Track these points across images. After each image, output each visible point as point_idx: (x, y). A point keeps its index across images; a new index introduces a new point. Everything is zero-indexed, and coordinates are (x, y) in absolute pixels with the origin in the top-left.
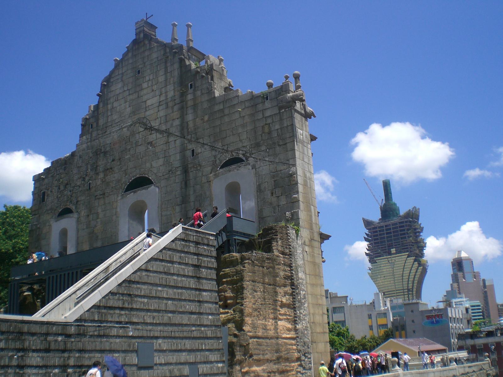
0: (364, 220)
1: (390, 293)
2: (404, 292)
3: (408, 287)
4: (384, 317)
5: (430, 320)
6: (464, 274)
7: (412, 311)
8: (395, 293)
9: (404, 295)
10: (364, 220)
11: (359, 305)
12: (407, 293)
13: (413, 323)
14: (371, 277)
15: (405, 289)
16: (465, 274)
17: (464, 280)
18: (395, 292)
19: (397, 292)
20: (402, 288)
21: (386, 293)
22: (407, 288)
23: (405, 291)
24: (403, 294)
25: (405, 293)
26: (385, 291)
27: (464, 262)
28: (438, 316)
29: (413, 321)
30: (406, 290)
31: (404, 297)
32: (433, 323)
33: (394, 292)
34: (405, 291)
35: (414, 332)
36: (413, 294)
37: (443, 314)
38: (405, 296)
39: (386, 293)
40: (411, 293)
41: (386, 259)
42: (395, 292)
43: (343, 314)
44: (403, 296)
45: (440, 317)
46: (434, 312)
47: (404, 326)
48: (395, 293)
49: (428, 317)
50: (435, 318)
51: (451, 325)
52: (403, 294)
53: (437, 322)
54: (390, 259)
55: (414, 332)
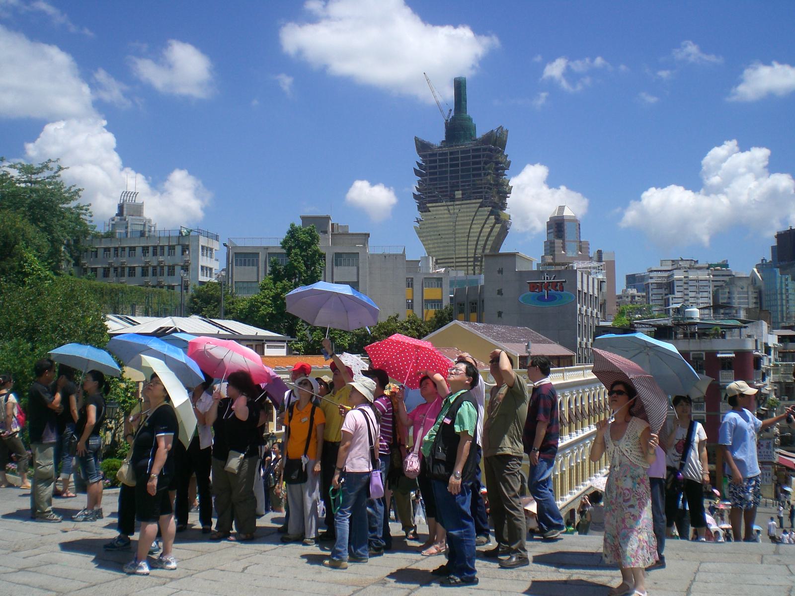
0: (417, 140)
1: (447, 261)
2: (468, 262)
3: (475, 254)
4: (438, 287)
5: (536, 293)
6: (563, 243)
7: (501, 271)
8: (453, 262)
9: (468, 266)
10: (417, 140)
11: (390, 255)
12: (472, 264)
13: (499, 296)
14: (418, 233)
15: (470, 257)
16: (567, 243)
17: (563, 252)
18: (454, 260)
19: (458, 260)
20: (466, 256)
22: (473, 255)
23: (469, 260)
24: (466, 264)
25: (469, 264)
27: (566, 223)
28: (555, 285)
29: (500, 292)
30: (472, 259)
31: (468, 270)
32: (541, 299)
33: (451, 260)
34: (469, 260)
35: (500, 314)
36: (481, 266)
37: (565, 282)
38: (469, 268)
40: (479, 264)
41: (446, 208)
42: (454, 260)
43: (355, 268)
44: (466, 268)
45: (558, 288)
46: (546, 276)
47: (476, 304)
48: (453, 262)
49: (533, 287)
50: (547, 288)
51: (579, 306)
52: (466, 264)
53: (551, 298)
54: (451, 207)
55: (500, 314)
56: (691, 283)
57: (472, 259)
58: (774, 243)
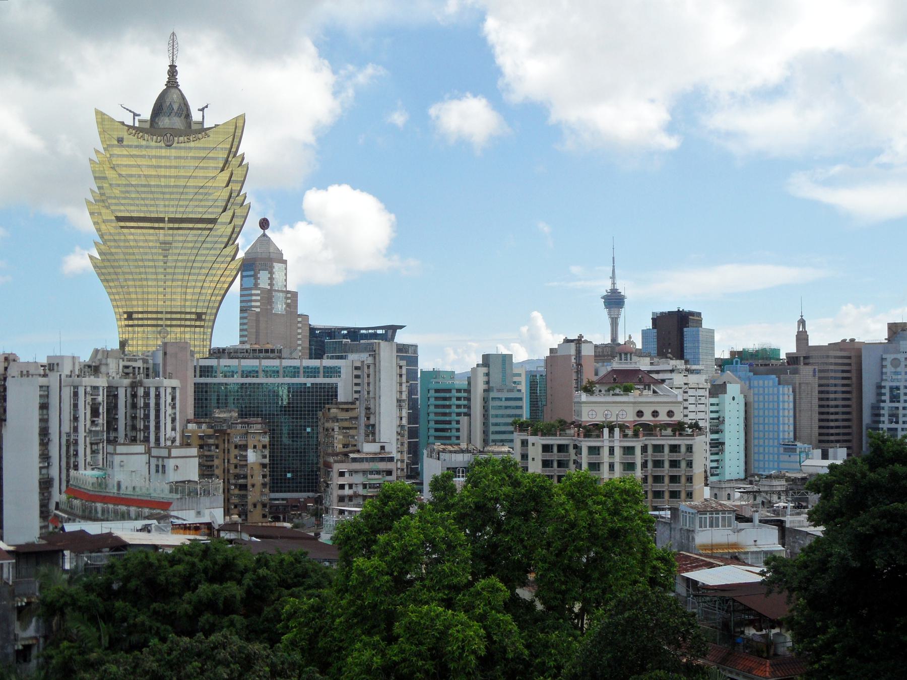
1: (150, 316)
12: (193, 323)
14: (95, 267)
16: (274, 294)
19: (169, 316)
21: (135, 316)
26: (135, 309)
27: (275, 264)
30: (193, 316)
33: (160, 316)
34: (188, 316)
39: (135, 316)
40: (202, 323)
41: (152, 231)
48: (161, 319)
54: (162, 231)
56: (691, 392)
57: (193, 316)
58: (649, 325)
